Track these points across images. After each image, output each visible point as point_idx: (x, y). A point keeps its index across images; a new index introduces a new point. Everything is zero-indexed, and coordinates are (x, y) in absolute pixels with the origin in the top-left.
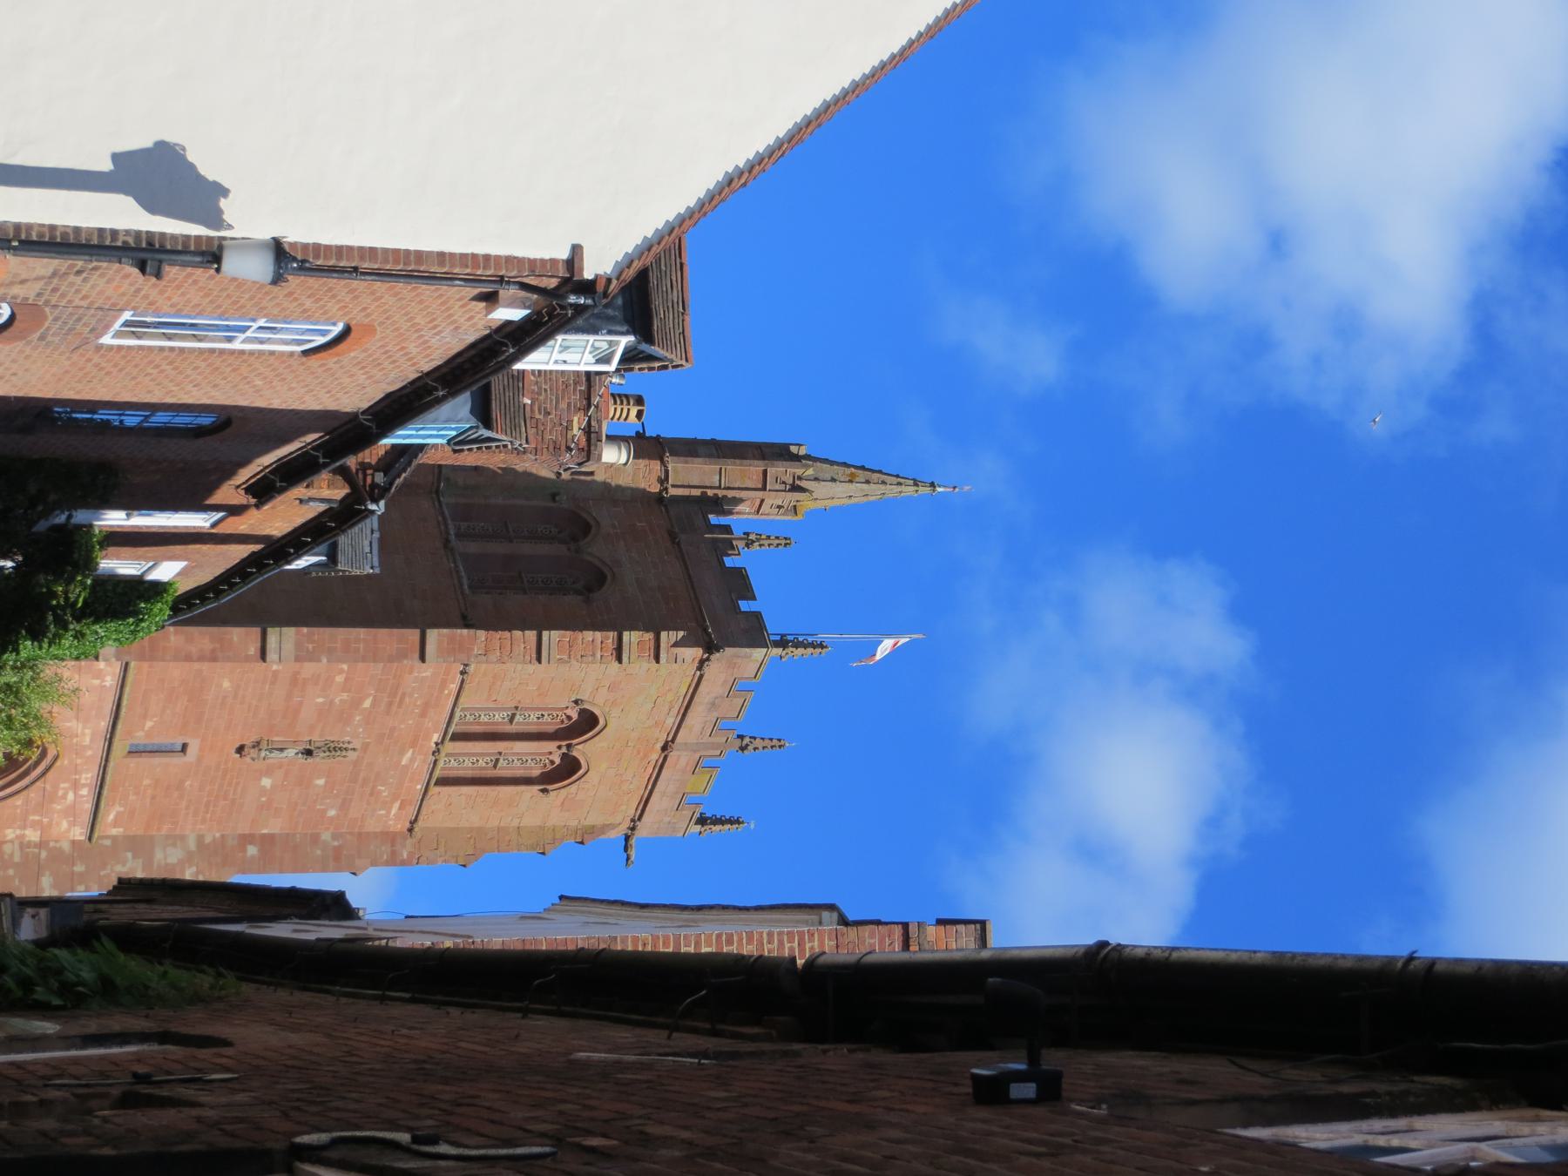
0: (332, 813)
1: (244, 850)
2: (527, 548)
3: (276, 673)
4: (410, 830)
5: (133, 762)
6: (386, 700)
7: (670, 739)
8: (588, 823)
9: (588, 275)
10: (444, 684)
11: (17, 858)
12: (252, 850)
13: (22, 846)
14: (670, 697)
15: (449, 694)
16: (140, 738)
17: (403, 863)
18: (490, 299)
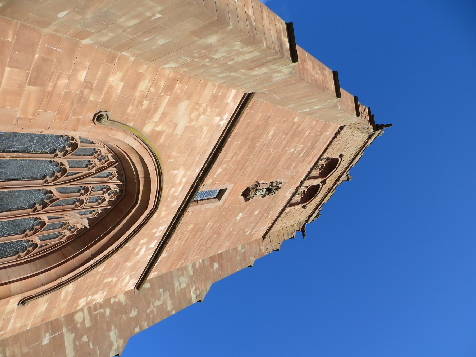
1: (213, 267)
11: (88, 324)
13: (90, 310)
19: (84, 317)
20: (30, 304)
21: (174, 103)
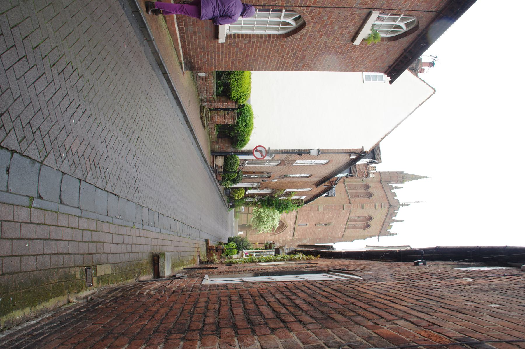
0: (330, 234)
2: (359, 191)
3: (320, 212)
4: (343, 236)
5: (299, 227)
8: (372, 234)
9: (365, 151)
11: (282, 242)
12: (318, 240)
14: (384, 214)
16: (300, 223)
17: (342, 242)
18: (350, 155)
20: (271, 236)
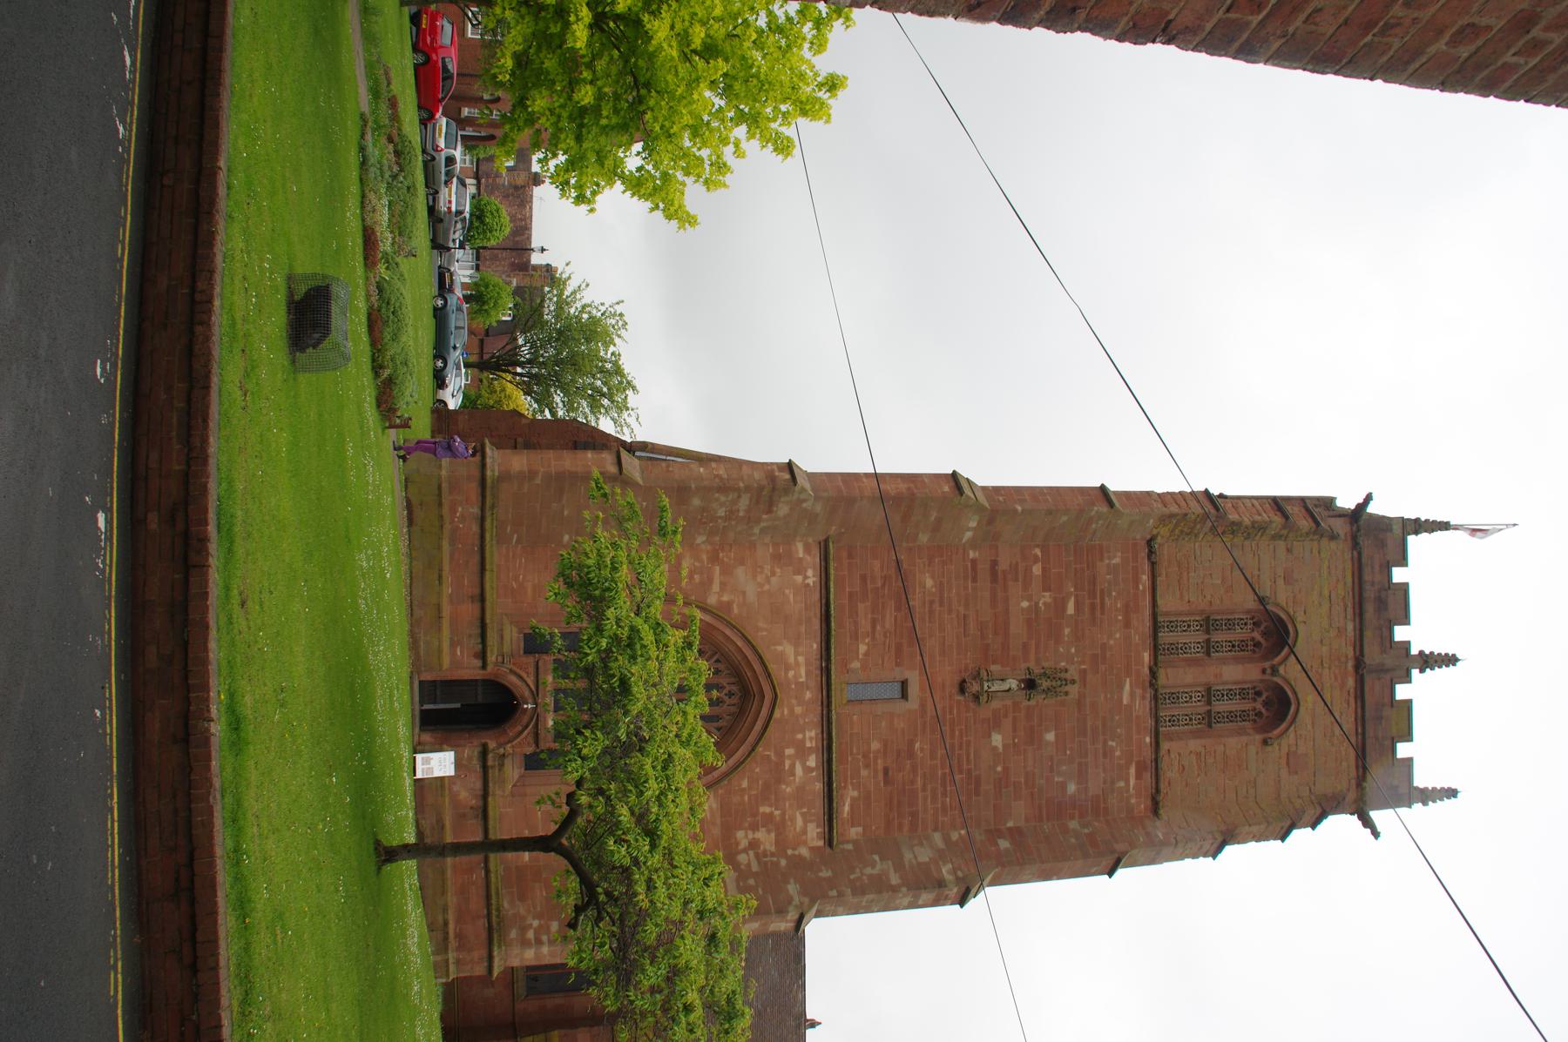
3: (974, 561)
6: (1087, 602)
7: (1358, 653)
10: (1136, 581)
11: (755, 867)
15: (1144, 587)
19: (749, 860)
21: (726, 571)
